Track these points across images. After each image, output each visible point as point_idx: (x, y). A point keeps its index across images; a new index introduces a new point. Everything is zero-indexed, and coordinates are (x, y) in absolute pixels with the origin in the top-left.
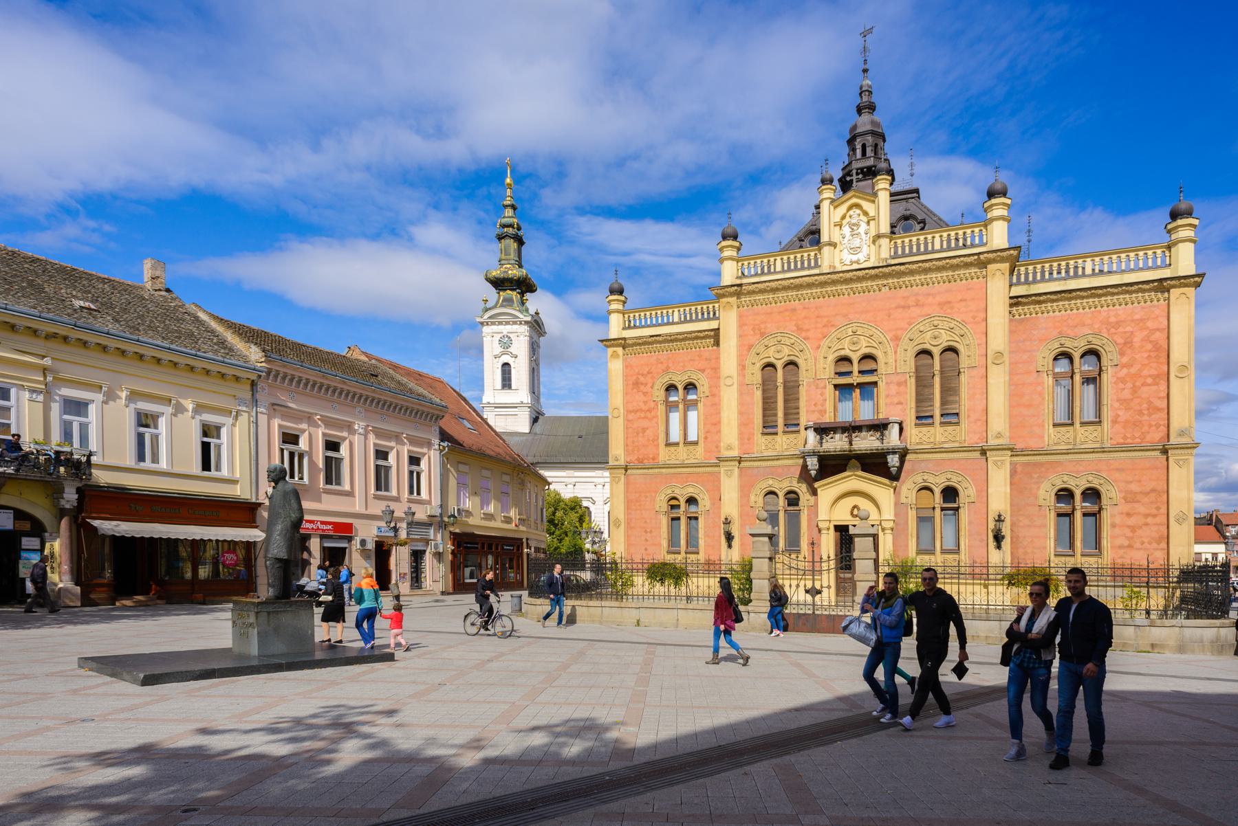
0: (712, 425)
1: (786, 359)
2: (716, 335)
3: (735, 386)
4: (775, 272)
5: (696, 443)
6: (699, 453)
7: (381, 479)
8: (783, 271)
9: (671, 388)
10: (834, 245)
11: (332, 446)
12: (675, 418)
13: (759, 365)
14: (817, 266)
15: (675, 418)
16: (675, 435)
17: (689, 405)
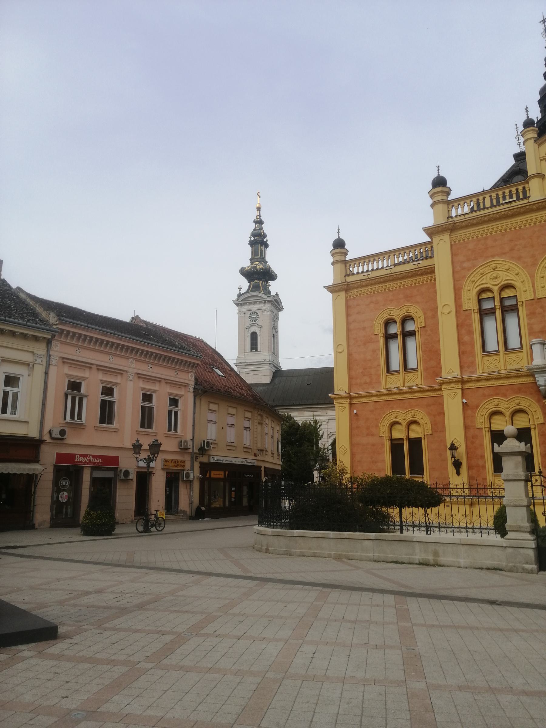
0: (432, 353)
1: (503, 283)
2: (431, 271)
3: (453, 313)
4: (485, 208)
5: (415, 370)
6: (416, 380)
7: (147, 418)
8: (492, 206)
9: (388, 323)
10: (541, 176)
11: (108, 391)
12: (395, 348)
13: (475, 291)
14: (525, 197)
15: (395, 348)
16: (396, 363)
17: (407, 335)
